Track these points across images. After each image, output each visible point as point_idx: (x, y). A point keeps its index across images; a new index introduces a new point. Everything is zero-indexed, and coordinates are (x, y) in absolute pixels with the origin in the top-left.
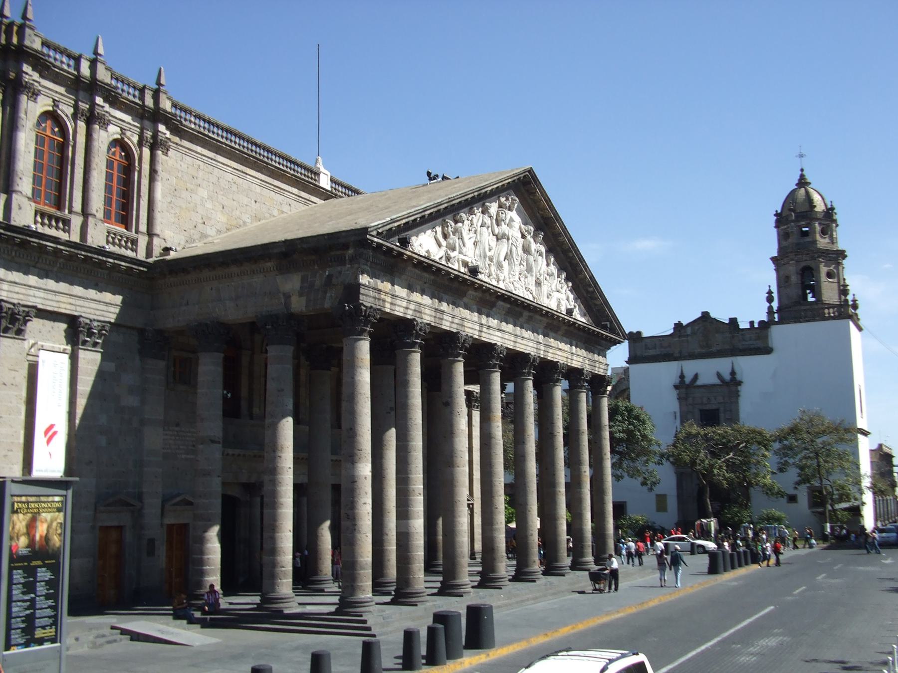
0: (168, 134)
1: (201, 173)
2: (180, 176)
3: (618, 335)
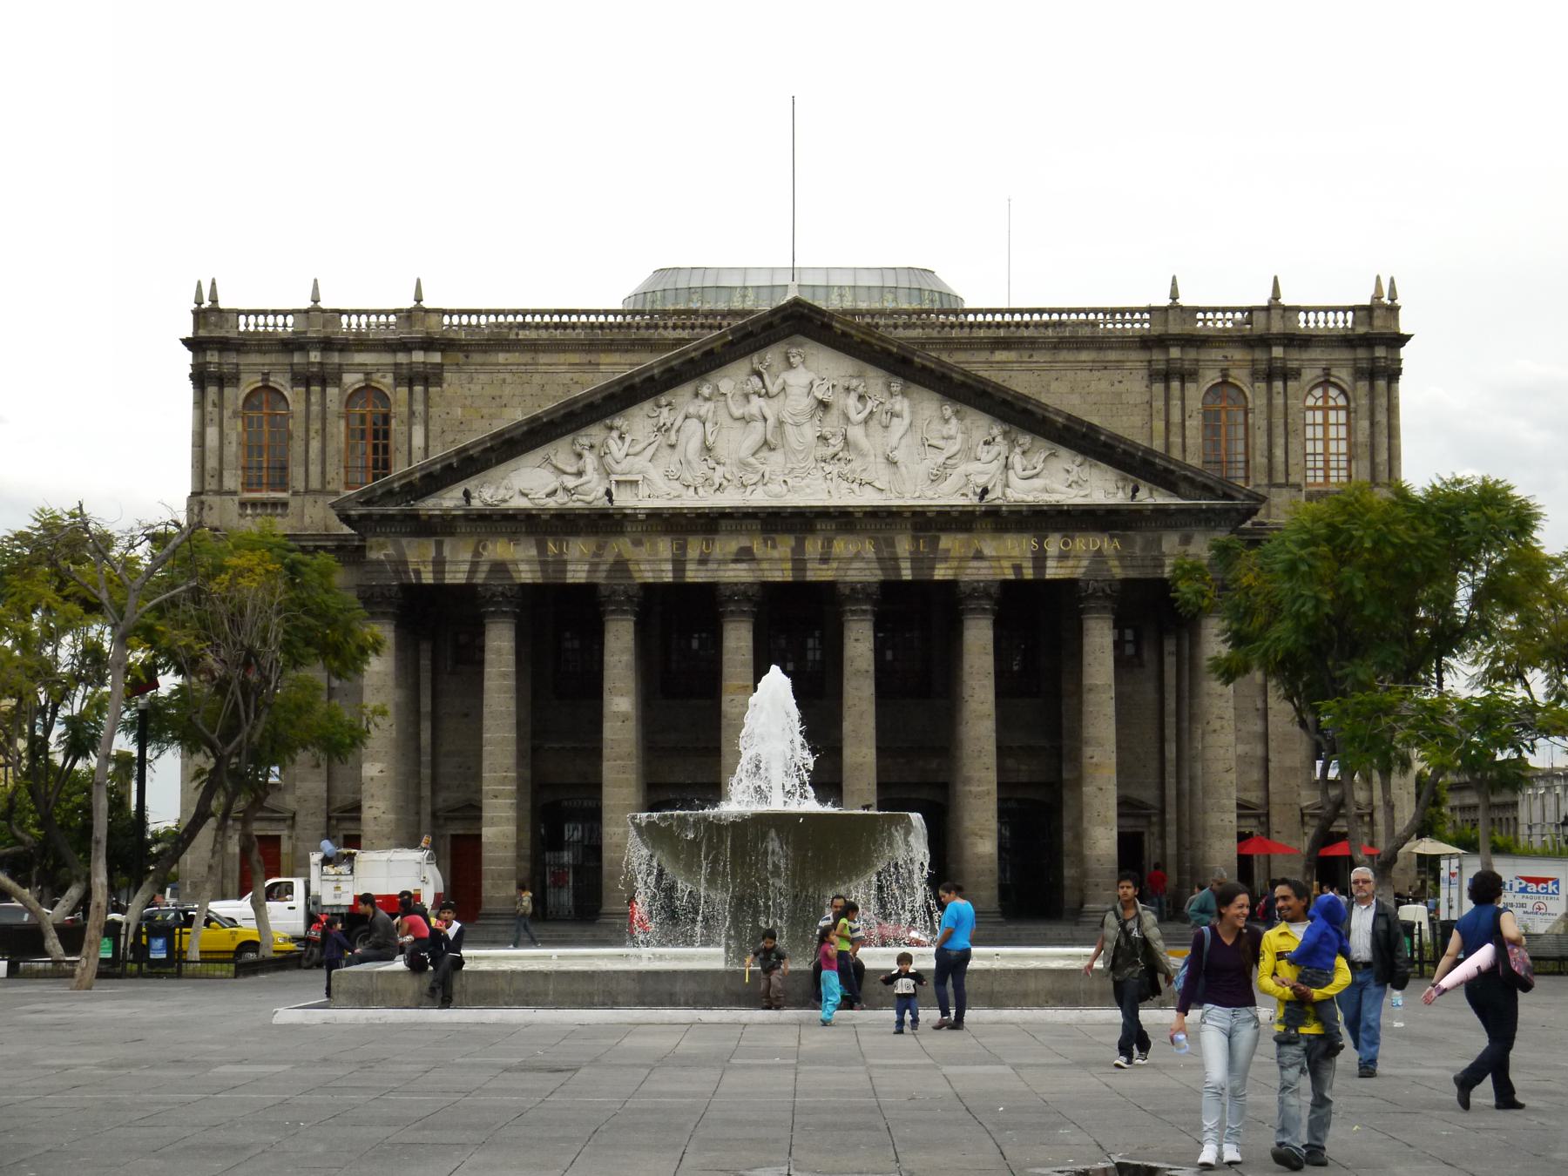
0: (436, 358)
1: (507, 390)
2: (468, 402)
3: (1227, 496)
